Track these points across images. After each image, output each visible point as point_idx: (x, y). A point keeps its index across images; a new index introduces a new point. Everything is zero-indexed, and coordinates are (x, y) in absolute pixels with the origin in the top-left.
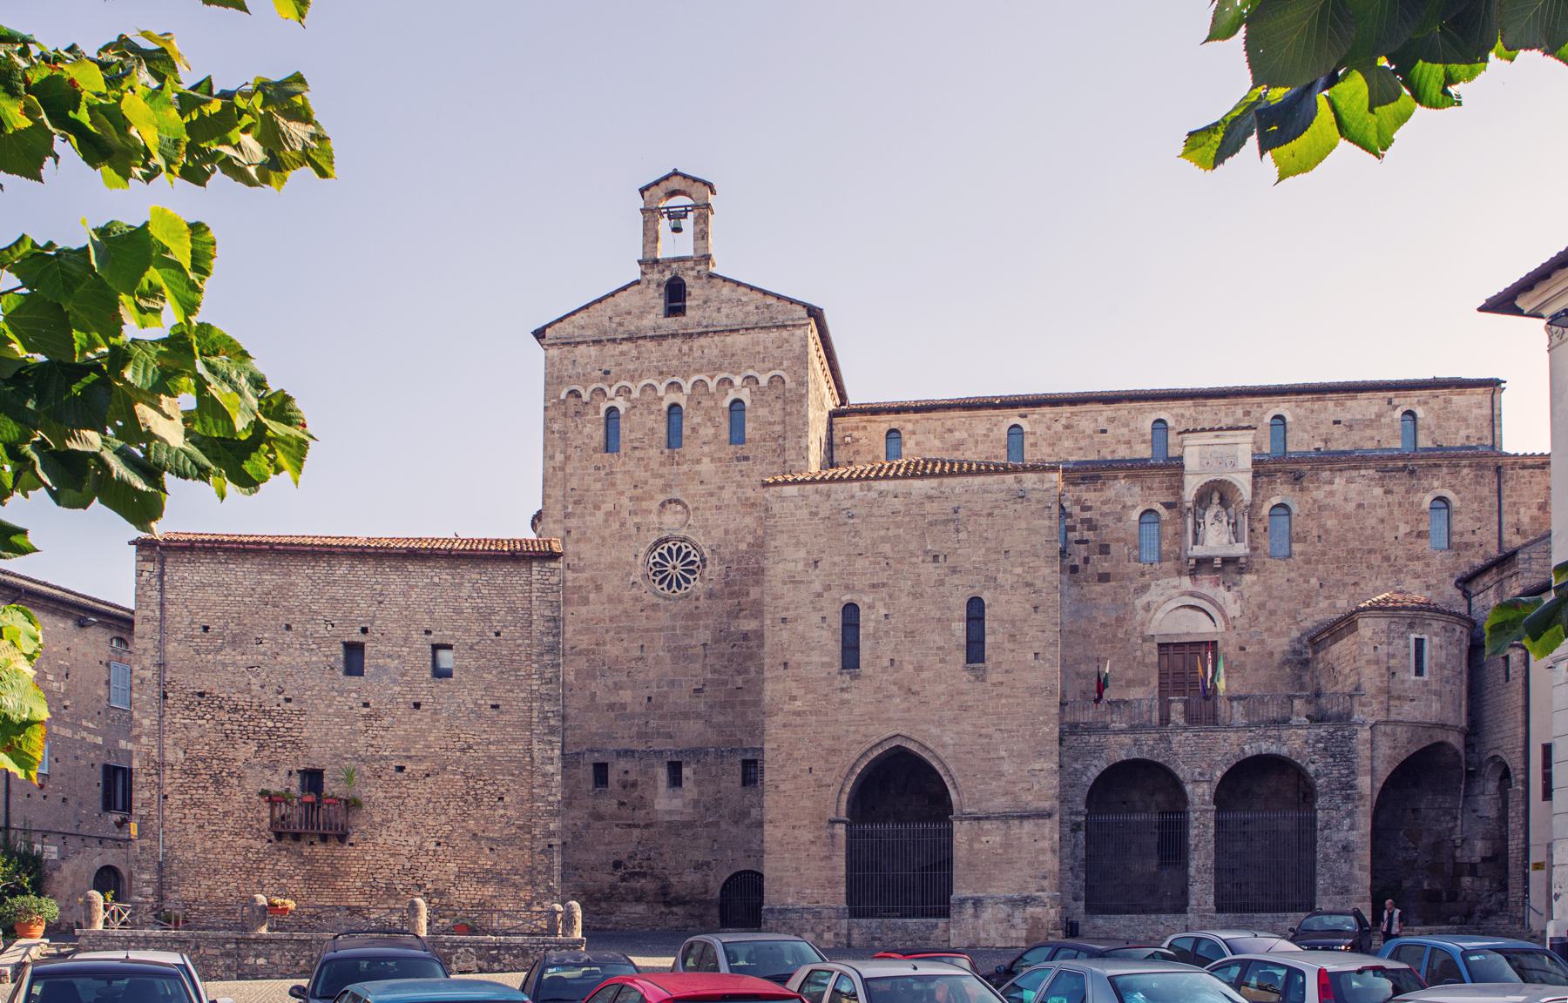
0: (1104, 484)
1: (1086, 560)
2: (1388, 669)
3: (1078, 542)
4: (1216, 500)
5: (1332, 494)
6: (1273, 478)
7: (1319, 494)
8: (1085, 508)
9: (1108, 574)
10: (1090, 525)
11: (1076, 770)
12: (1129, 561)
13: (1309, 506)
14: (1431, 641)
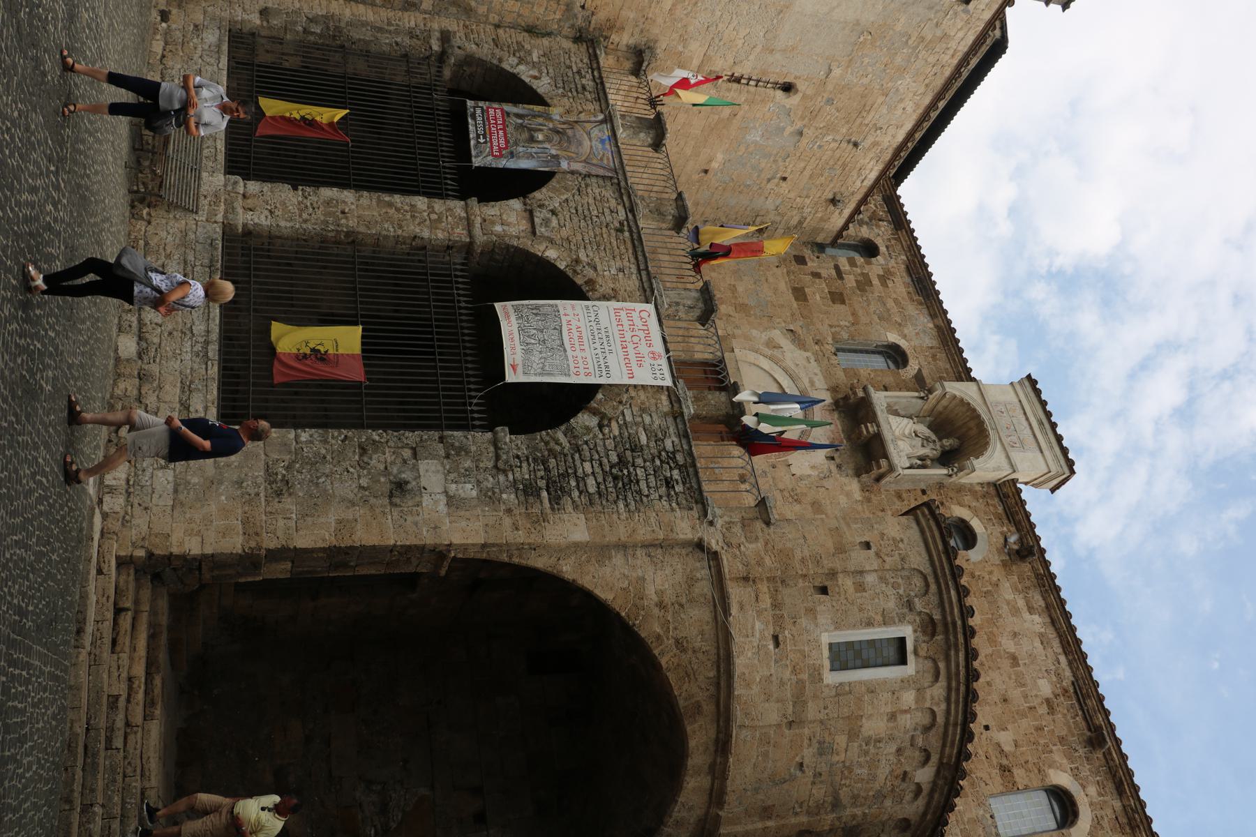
0: (921, 304)
1: (817, 275)
2: (833, 574)
3: (837, 268)
4: (947, 443)
5: (1015, 611)
6: (1006, 521)
7: (1007, 592)
8: (884, 279)
9: (806, 299)
10: (864, 284)
11: (529, 53)
12: (831, 326)
13: (987, 577)
14: (905, 683)
